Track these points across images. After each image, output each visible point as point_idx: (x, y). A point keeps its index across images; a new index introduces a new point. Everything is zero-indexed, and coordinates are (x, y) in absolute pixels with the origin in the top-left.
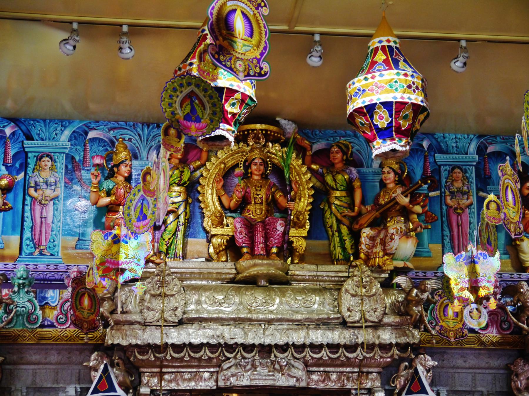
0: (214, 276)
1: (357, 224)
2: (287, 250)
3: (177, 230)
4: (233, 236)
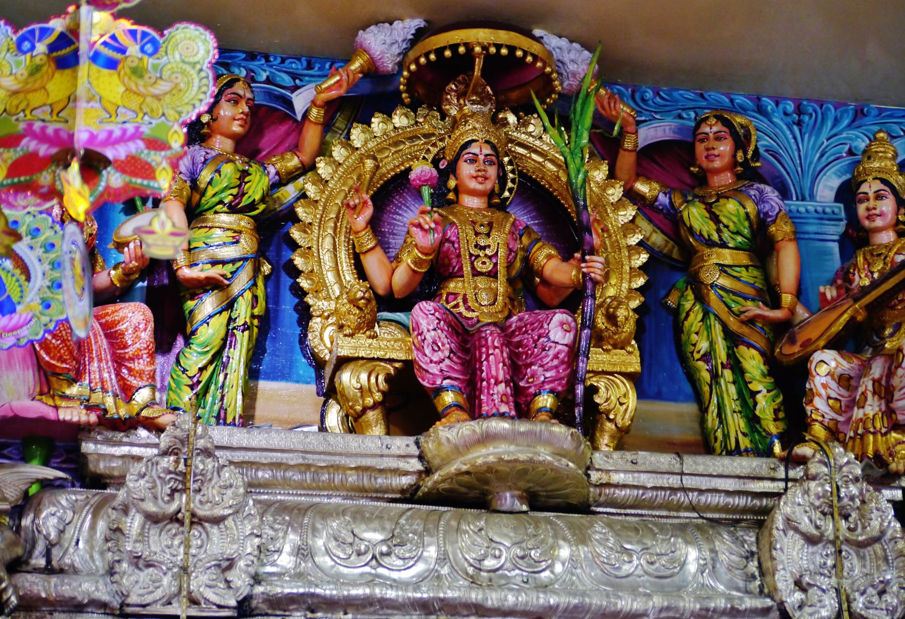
0: (352, 478)
1: (792, 341)
2: (580, 411)
3: (227, 339)
4: (409, 364)
